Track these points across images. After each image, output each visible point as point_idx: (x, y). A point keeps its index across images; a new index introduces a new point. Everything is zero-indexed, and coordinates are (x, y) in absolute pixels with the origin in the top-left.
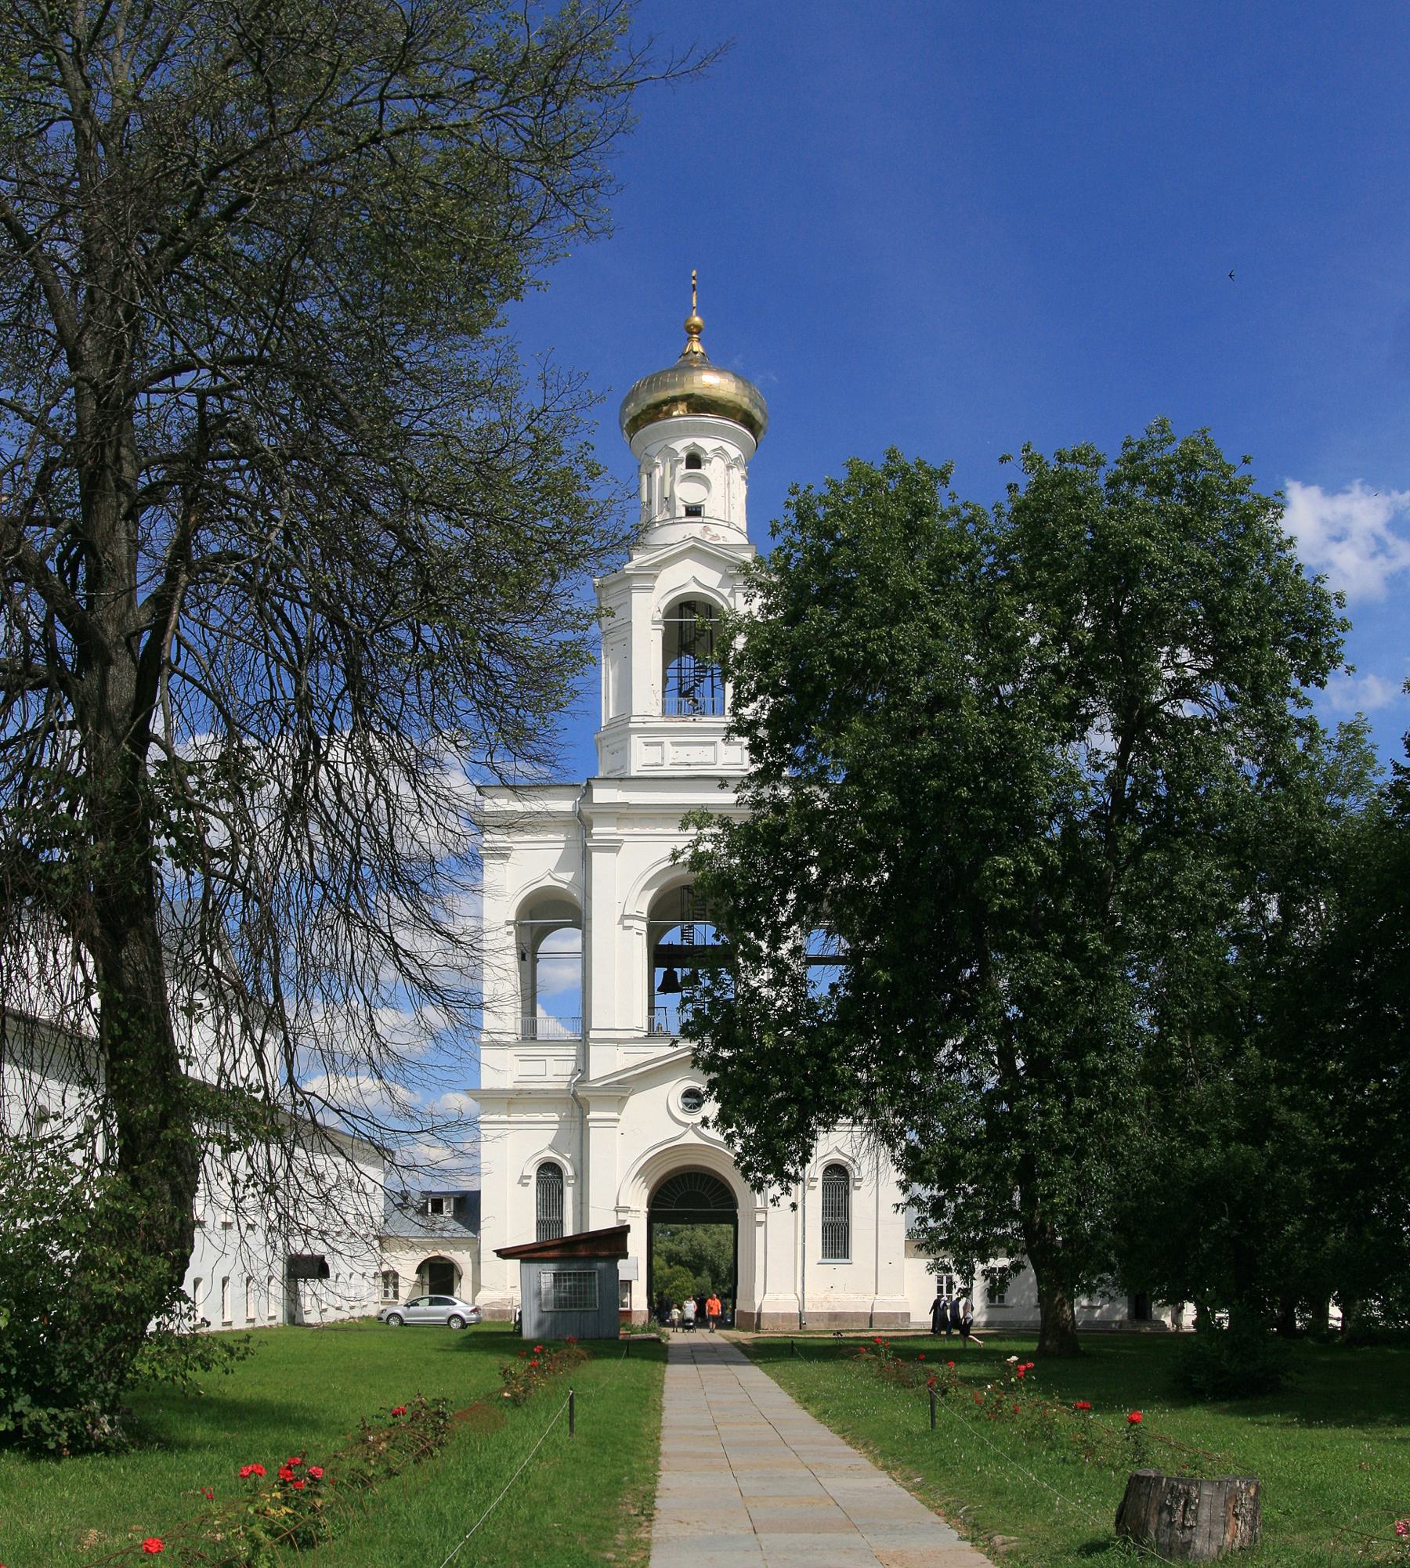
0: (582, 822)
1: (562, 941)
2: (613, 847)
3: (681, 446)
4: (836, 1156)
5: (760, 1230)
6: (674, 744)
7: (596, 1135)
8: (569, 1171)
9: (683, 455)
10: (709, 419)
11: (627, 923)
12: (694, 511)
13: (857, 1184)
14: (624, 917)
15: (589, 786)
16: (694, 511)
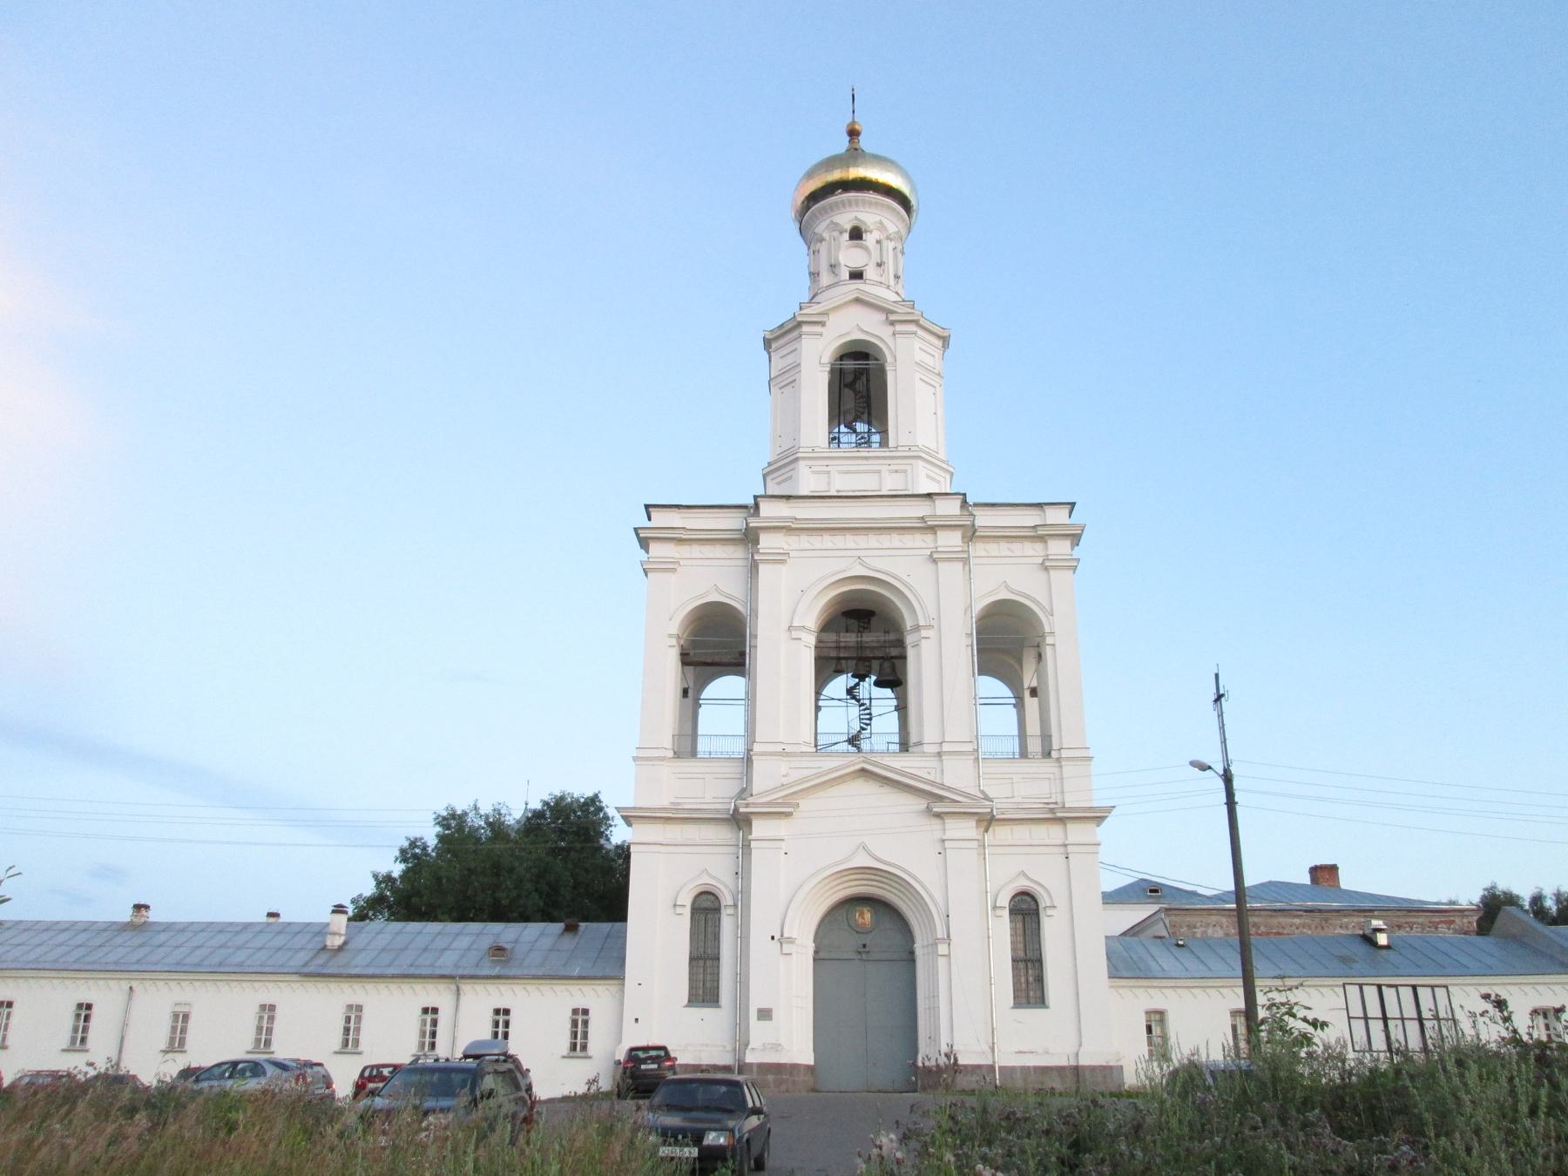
0: (749, 538)
1: (726, 686)
2: (780, 559)
3: (846, 220)
4: (1022, 884)
5: (942, 962)
6: (840, 472)
7: (760, 855)
8: (726, 899)
9: (848, 227)
10: (871, 196)
11: (795, 634)
12: (857, 275)
13: (1049, 912)
14: (790, 628)
15: (757, 506)
16: (857, 275)
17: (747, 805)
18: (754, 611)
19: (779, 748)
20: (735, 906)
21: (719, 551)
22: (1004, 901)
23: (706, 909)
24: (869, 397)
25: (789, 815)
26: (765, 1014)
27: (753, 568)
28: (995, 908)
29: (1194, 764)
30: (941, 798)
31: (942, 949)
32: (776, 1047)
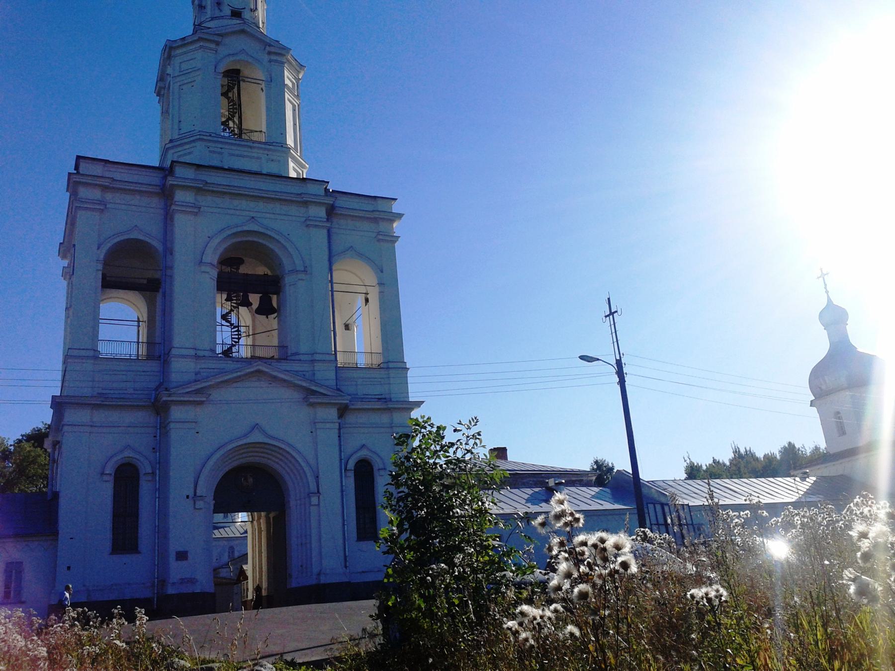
0: (166, 193)
4: (363, 454)
5: (314, 510)
7: (176, 434)
8: (145, 468)
11: (204, 268)
13: (382, 473)
17: (170, 395)
18: (169, 251)
19: (192, 352)
20: (153, 473)
21: (136, 200)
22: (351, 465)
23: (126, 478)
24: (240, 105)
25: (201, 403)
26: (182, 556)
27: (168, 218)
28: (346, 469)
29: (582, 358)
30: (314, 393)
31: (314, 500)
32: (192, 581)
